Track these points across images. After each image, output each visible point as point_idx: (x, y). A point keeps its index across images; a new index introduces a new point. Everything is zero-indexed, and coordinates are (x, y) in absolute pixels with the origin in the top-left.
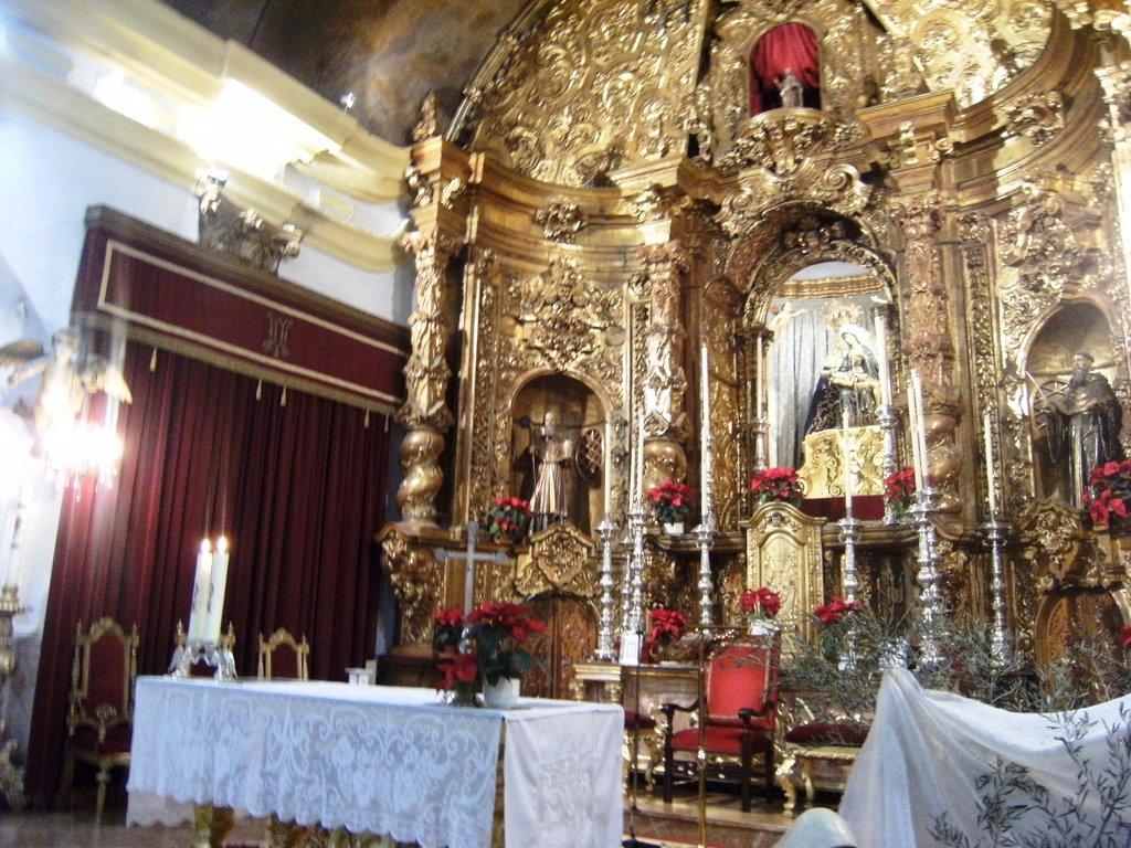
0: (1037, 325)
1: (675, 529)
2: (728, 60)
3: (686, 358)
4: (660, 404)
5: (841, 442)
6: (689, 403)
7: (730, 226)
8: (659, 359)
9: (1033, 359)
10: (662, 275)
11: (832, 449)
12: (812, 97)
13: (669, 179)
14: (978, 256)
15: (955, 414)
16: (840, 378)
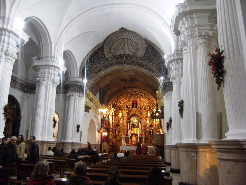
0: (149, 125)
1: (127, 136)
2: (131, 102)
3: (127, 125)
4: (125, 127)
5: (135, 129)
6: (127, 128)
7: (130, 114)
8: (126, 124)
9: (149, 127)
10: (126, 118)
11: (134, 129)
12: (136, 107)
13: (127, 112)
14: (146, 120)
15: (145, 130)
16: (135, 124)
